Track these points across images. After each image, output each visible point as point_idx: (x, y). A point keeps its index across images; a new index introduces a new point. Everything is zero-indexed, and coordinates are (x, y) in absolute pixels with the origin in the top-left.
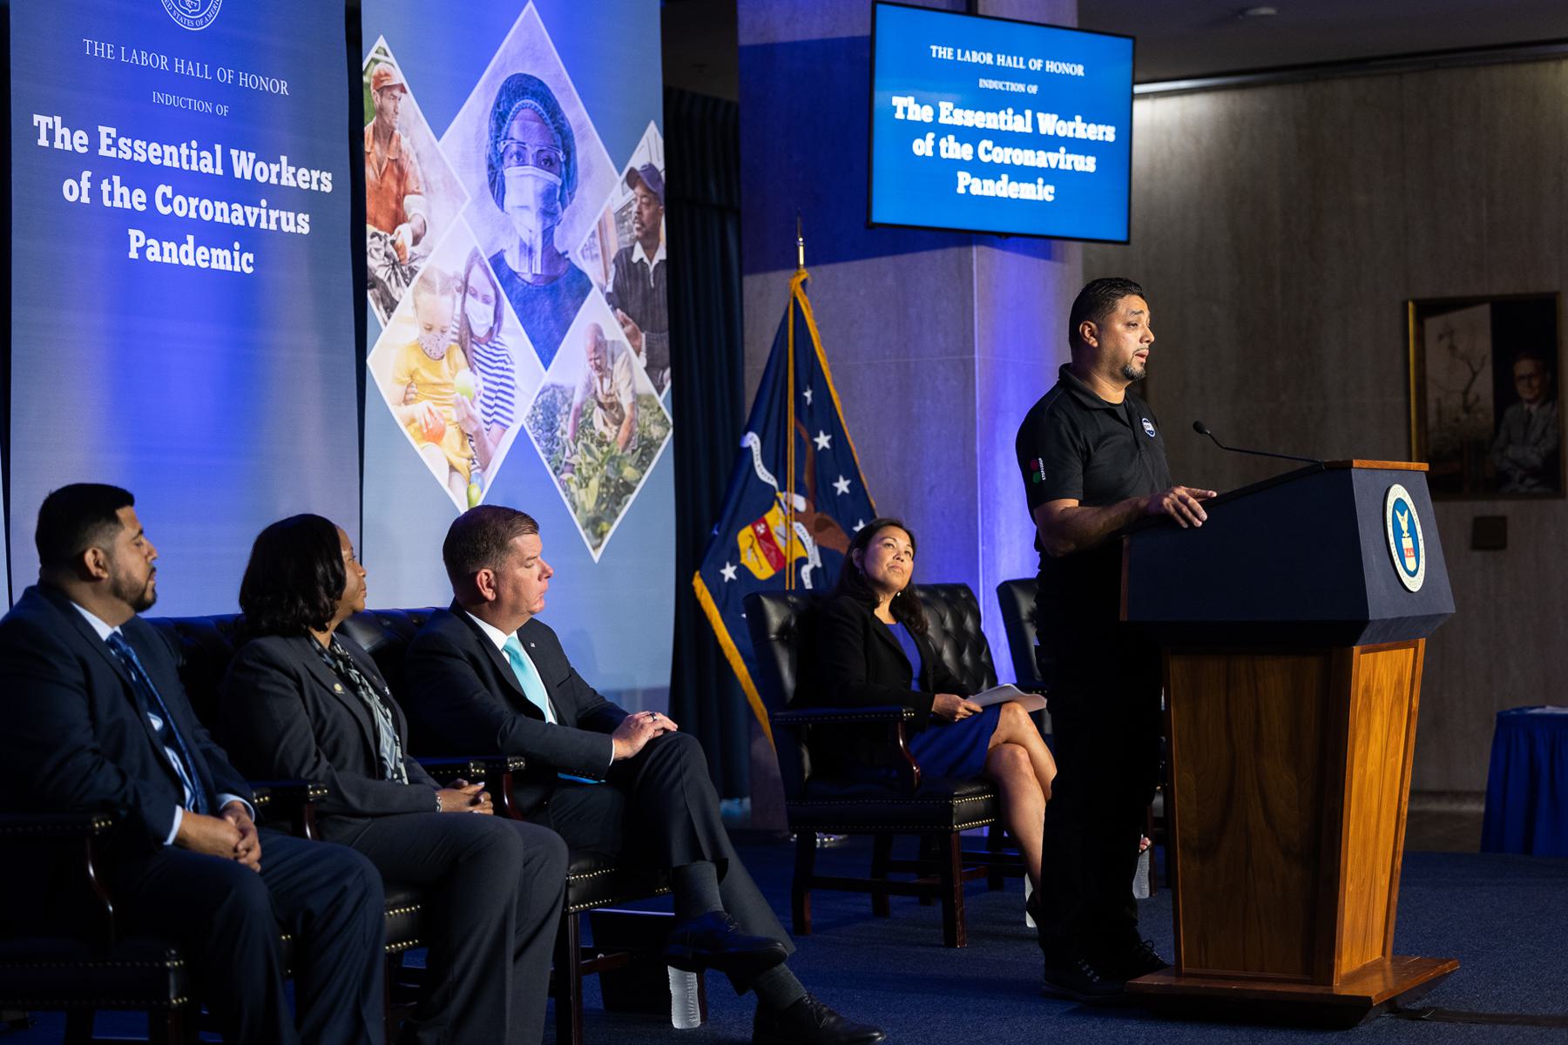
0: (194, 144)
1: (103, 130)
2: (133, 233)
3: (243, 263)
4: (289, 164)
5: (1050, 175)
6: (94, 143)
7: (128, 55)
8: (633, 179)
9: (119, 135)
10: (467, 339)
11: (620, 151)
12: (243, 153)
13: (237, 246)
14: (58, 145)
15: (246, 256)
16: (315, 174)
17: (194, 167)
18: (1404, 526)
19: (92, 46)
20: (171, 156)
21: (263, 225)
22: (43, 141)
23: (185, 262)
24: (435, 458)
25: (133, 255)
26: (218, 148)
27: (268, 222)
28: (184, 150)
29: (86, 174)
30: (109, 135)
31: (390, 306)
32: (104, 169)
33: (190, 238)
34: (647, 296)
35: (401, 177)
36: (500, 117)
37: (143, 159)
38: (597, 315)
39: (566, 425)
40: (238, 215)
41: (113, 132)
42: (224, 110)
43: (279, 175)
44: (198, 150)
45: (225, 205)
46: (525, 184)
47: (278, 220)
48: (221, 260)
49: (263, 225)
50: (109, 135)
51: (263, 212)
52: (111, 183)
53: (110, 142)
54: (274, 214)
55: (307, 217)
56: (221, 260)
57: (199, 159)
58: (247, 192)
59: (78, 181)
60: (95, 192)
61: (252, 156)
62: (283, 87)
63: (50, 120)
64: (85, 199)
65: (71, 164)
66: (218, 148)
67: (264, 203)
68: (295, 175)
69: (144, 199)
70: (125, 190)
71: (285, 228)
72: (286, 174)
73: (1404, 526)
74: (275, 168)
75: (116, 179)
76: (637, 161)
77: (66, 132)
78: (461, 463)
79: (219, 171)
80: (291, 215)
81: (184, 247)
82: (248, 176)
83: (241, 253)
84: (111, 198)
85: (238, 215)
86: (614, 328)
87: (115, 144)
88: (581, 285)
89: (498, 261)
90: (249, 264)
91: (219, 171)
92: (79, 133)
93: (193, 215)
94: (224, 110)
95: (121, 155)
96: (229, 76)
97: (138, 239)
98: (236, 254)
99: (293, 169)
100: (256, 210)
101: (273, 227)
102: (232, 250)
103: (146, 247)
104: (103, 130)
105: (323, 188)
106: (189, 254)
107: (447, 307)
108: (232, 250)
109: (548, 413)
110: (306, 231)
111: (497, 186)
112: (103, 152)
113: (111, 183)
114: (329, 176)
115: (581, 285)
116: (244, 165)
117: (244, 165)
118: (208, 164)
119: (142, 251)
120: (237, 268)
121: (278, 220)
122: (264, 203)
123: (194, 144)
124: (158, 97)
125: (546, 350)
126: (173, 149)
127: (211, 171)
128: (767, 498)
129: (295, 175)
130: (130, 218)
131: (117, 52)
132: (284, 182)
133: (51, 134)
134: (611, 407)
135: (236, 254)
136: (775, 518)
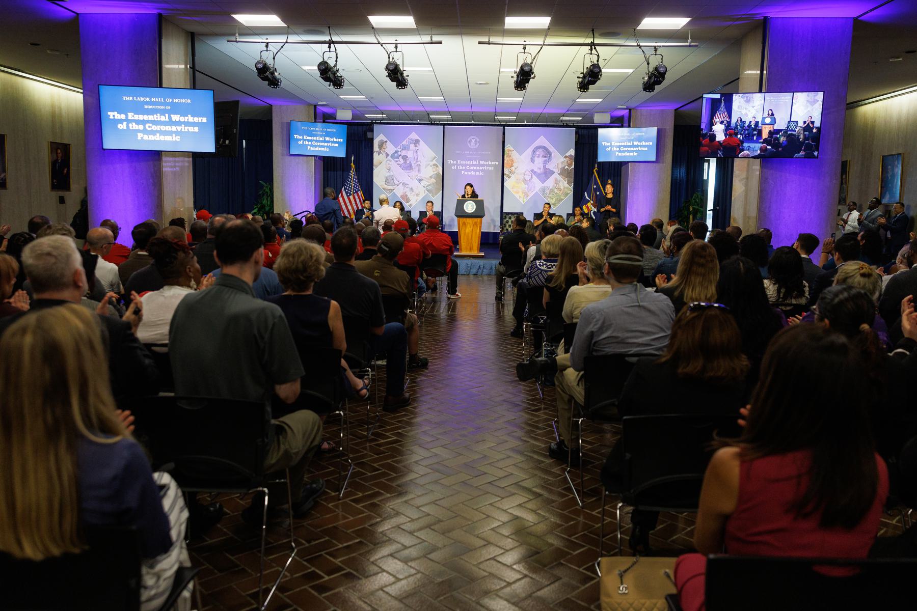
5: (636, 151)
8: (566, 157)
10: (525, 181)
11: (562, 153)
24: (517, 196)
31: (509, 177)
34: (568, 173)
35: (513, 161)
36: (534, 152)
38: (556, 176)
39: (547, 192)
46: (539, 161)
48: (478, 173)
56: (478, 173)
65: (454, 165)
76: (567, 154)
78: (522, 196)
86: (560, 178)
88: (553, 173)
89: (532, 171)
106: (472, 173)
107: (521, 177)
109: (543, 190)
111: (532, 160)
115: (553, 173)
116: (482, 162)
117: (482, 162)
125: (543, 182)
128: (588, 201)
134: (559, 189)
136: (589, 204)
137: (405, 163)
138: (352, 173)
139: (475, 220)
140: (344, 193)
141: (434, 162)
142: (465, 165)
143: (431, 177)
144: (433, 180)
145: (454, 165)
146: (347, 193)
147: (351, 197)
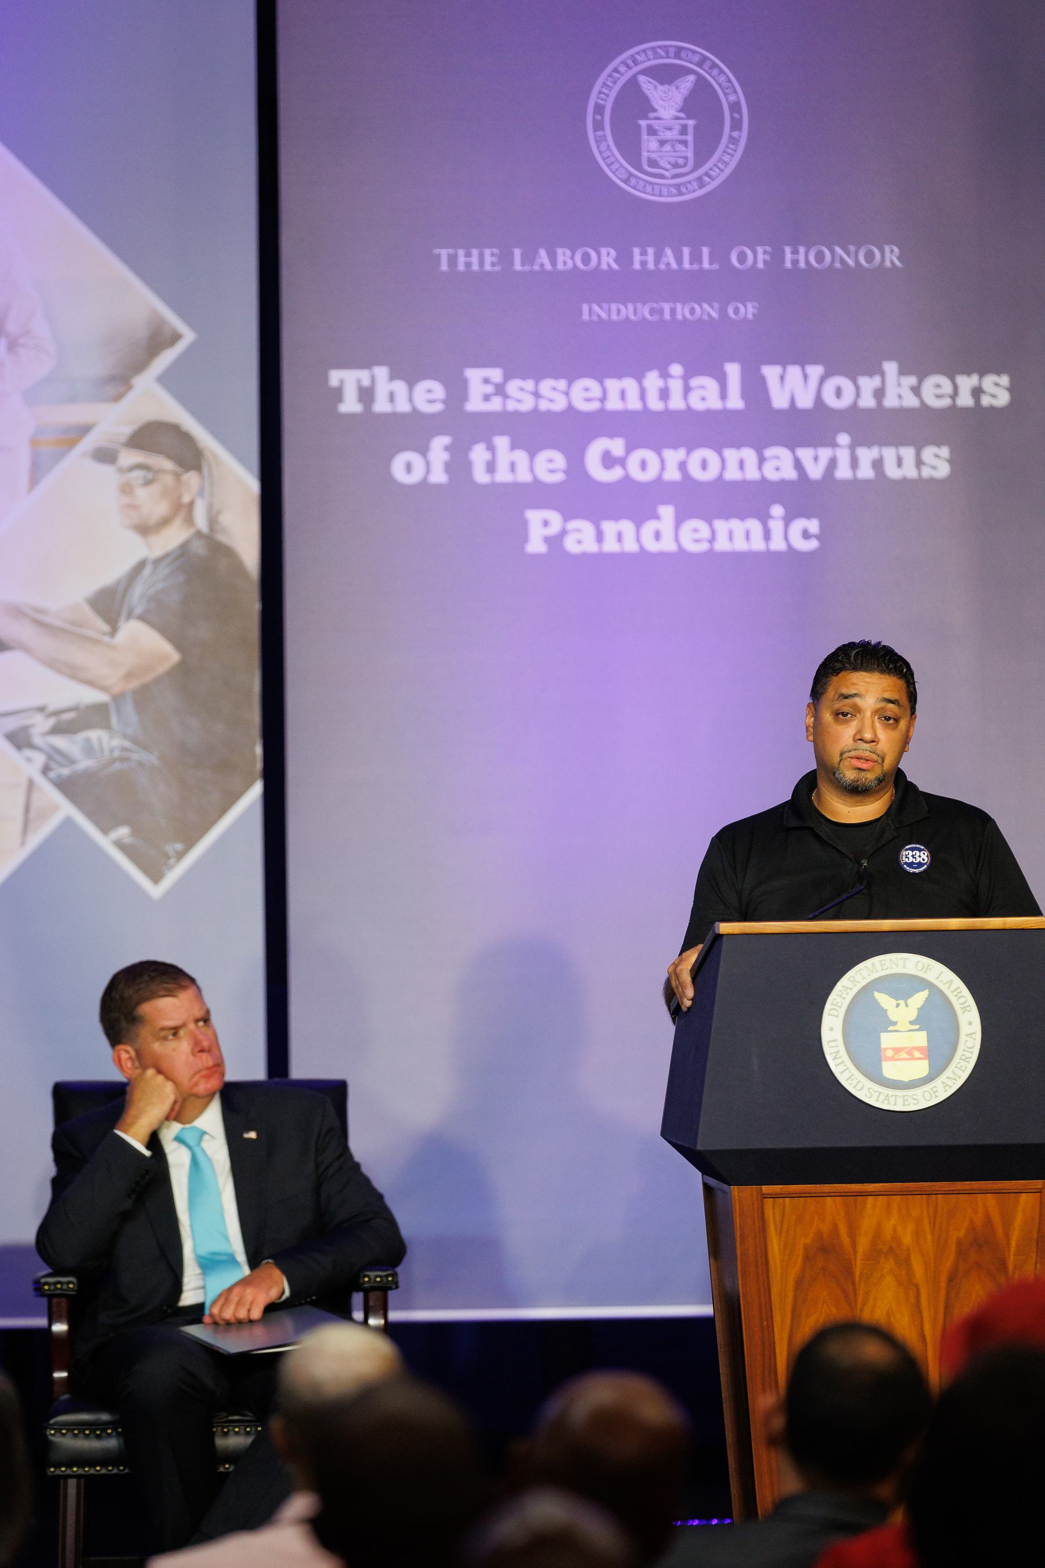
0: (676, 369)
1: (474, 376)
2: (534, 517)
3: (800, 535)
4: (902, 372)
6: (457, 391)
7: (529, 257)
9: (507, 378)
12: (794, 372)
13: (777, 510)
14: (381, 406)
15: (799, 525)
16: (966, 383)
17: (676, 403)
18: (902, 1012)
19: (453, 260)
20: (622, 394)
21: (843, 472)
22: (350, 405)
23: (651, 546)
25: (536, 545)
26: (733, 371)
27: (854, 463)
28: (653, 381)
29: (439, 445)
30: (486, 381)
32: (466, 429)
33: (667, 512)
37: (559, 404)
40: (780, 464)
41: (496, 374)
42: (749, 310)
43: (879, 394)
44: (686, 378)
45: (749, 455)
47: (878, 464)
48: (738, 535)
49: (843, 472)
50: (486, 381)
51: (843, 456)
52: (491, 448)
53: (489, 389)
54: (866, 455)
55: (945, 452)
56: (738, 535)
57: (687, 390)
58: (809, 426)
59: (423, 451)
60: (458, 464)
61: (815, 371)
62: (891, 256)
63: (364, 376)
64: (438, 476)
65: (413, 430)
66: (733, 371)
67: (844, 439)
68: (916, 391)
69: (559, 460)
70: (521, 457)
71: (892, 471)
72: (897, 388)
73: (902, 1012)
74: (868, 384)
75: (502, 442)
77: (400, 387)
79: (735, 402)
80: (908, 453)
81: (649, 528)
82: (805, 401)
83: (788, 520)
84: (491, 467)
85: (780, 464)
87: (500, 390)
90: (806, 535)
91: (735, 402)
92: (422, 386)
93: (672, 474)
94: (749, 310)
95: (511, 406)
96: (760, 257)
97: (546, 523)
98: (776, 526)
99: (912, 380)
100: (825, 454)
101: (866, 472)
102: (764, 518)
103: (564, 533)
104: (474, 376)
105: (986, 401)
106: (664, 533)
108: (764, 518)
110: (943, 470)
112: (475, 404)
113: (491, 448)
114: (1005, 380)
116: (791, 386)
118: (705, 395)
119: (555, 542)
120: (778, 544)
121: (878, 464)
122: (844, 439)
123: (676, 369)
124: (592, 312)
126: (630, 384)
127: (714, 403)
129: (916, 391)
130: (538, 494)
131: (505, 259)
132: (890, 401)
133: (366, 395)
135: (776, 526)
139: (976, 1203)
141: (151, 399)
142: (571, 431)
143: (109, 605)
144: (144, 644)
145: (413, 430)
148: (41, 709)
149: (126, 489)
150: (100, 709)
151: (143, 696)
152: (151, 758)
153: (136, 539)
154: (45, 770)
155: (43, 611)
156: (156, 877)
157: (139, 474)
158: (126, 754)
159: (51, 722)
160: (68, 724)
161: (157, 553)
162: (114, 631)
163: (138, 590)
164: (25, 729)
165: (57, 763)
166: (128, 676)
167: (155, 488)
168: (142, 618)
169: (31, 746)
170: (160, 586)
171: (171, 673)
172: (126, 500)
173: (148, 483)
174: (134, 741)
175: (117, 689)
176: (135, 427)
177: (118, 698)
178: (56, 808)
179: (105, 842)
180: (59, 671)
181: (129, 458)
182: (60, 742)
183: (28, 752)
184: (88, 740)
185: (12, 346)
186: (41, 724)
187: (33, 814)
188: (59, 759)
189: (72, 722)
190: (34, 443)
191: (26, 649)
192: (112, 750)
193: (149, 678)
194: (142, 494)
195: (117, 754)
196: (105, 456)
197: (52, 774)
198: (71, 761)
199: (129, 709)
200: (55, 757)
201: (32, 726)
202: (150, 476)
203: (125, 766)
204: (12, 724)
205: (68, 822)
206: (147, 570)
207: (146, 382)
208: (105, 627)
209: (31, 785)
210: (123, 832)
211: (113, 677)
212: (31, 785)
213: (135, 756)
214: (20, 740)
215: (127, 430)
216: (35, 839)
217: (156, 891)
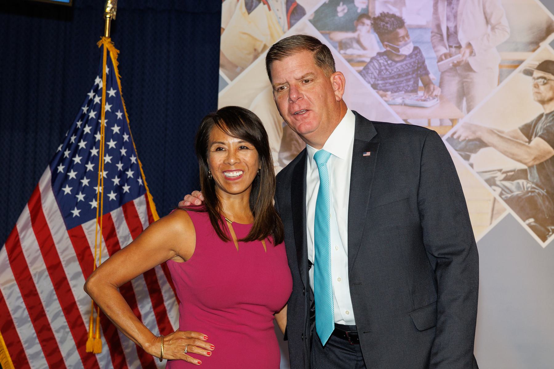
137: (390, 54)
138: (104, 92)
140: (49, 203)
143: (528, 131)
146: (66, 205)
147: (92, 230)
148: (500, 170)
149: (536, 86)
150: (524, 171)
151: (541, 167)
152: (543, 192)
153: (539, 105)
154: (501, 195)
155: (502, 132)
156: (544, 239)
157: (542, 80)
158: (533, 190)
159: (504, 175)
160: (512, 176)
161: (548, 111)
162: (530, 141)
163: (540, 125)
164: (494, 178)
165: (505, 192)
166: (535, 159)
167: (547, 86)
168: (540, 137)
169: (495, 185)
170: (548, 124)
171: (551, 159)
172: (536, 90)
173: (545, 84)
174: (537, 185)
175: (530, 164)
176: (540, 62)
177: (531, 167)
178: (505, 210)
179: (524, 224)
180: (508, 156)
181: (537, 74)
182: (507, 184)
183: (494, 187)
184: (518, 183)
185: (493, 29)
186: (500, 176)
187: (495, 212)
188: (507, 191)
189: (513, 175)
190: (501, 66)
191: (495, 147)
192: (527, 188)
193: (542, 161)
194: (542, 88)
195: (529, 189)
196: (529, 73)
197: (503, 197)
198: (512, 192)
199: (535, 172)
200: (505, 189)
201: (496, 177)
202: (545, 81)
203: (533, 194)
204: (488, 176)
205: (509, 215)
206: (544, 117)
207: (545, 45)
208: (527, 140)
209: (495, 199)
210: (531, 220)
211: (529, 159)
212: (495, 199)
213: (537, 191)
214: (491, 182)
215: (537, 63)
216: (496, 222)
217: (544, 245)
